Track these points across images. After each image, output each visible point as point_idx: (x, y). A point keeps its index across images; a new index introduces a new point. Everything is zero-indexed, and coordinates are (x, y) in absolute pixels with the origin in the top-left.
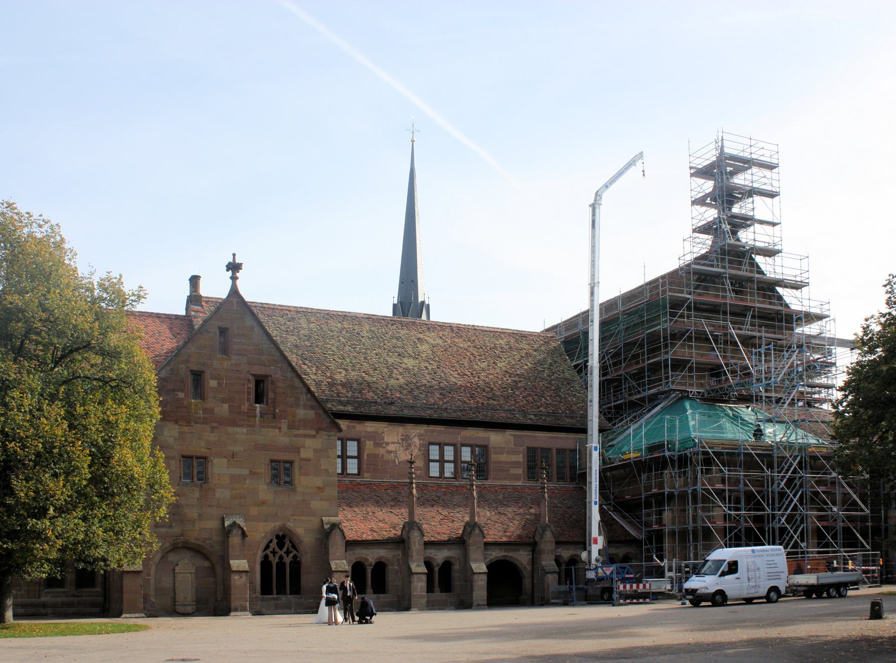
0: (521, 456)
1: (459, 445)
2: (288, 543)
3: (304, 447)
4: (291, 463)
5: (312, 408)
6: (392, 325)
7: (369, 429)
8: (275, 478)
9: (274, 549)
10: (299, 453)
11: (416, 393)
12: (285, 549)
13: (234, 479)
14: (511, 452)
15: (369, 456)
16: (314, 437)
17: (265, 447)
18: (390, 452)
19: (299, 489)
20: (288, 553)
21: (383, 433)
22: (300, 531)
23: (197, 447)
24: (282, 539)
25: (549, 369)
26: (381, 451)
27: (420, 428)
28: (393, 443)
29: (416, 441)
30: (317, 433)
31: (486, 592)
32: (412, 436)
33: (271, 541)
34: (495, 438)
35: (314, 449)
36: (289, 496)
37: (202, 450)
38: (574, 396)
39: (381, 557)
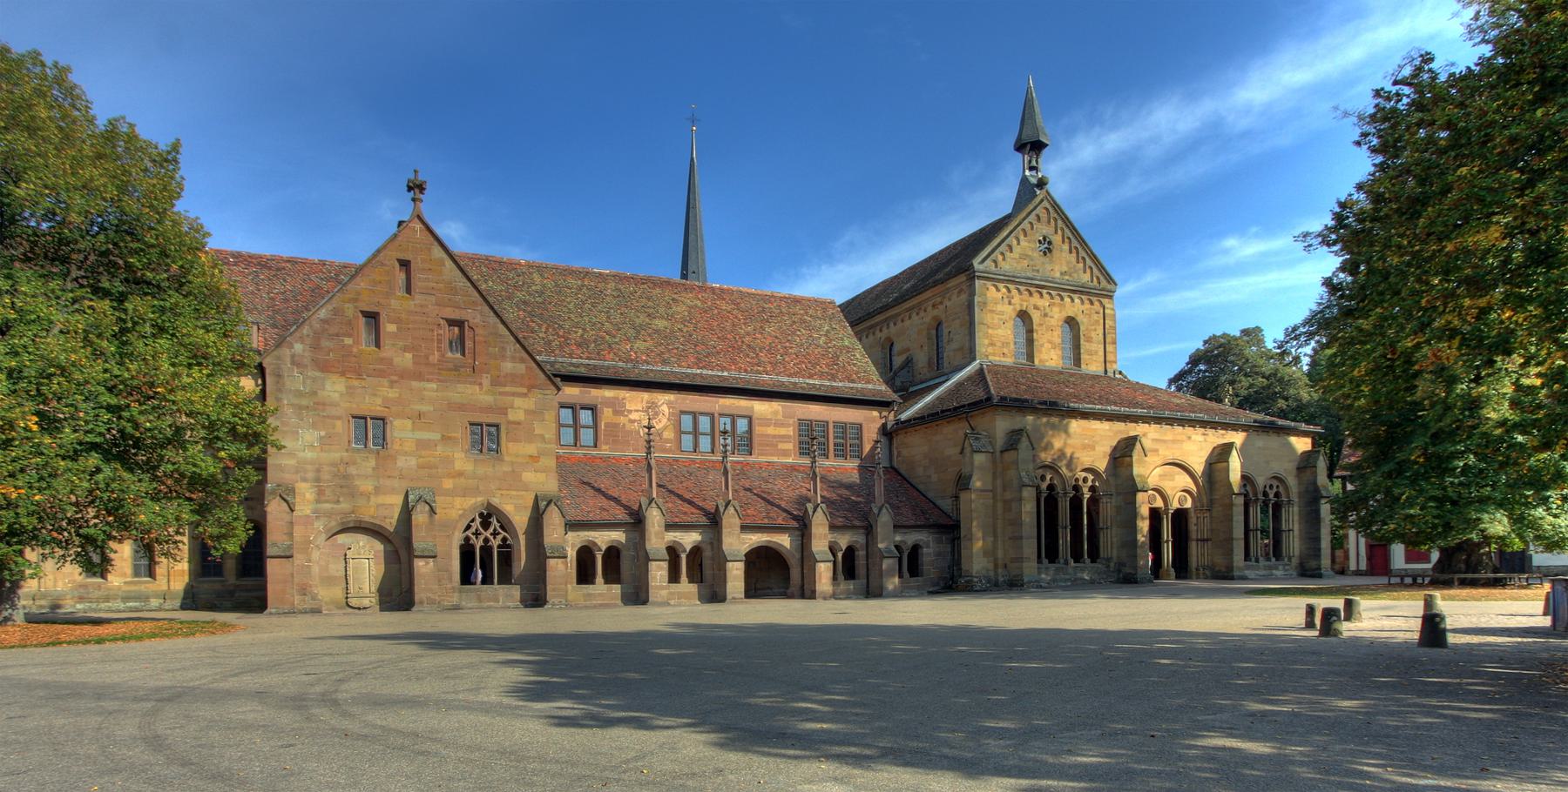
1: (716, 415)
3: (512, 407)
4: (497, 426)
5: (522, 360)
6: (643, 284)
9: (477, 530)
10: (506, 414)
11: (666, 356)
12: (491, 530)
13: (422, 445)
14: (778, 424)
15: (607, 425)
16: (525, 395)
17: (461, 407)
18: (633, 421)
19: (507, 458)
20: (495, 534)
22: (508, 508)
23: (371, 404)
24: (488, 516)
25: (826, 335)
26: (622, 420)
28: (637, 411)
30: (529, 390)
31: (743, 584)
33: (473, 521)
34: (760, 407)
35: (525, 411)
36: (494, 466)
37: (378, 408)
38: (854, 365)
39: (613, 541)
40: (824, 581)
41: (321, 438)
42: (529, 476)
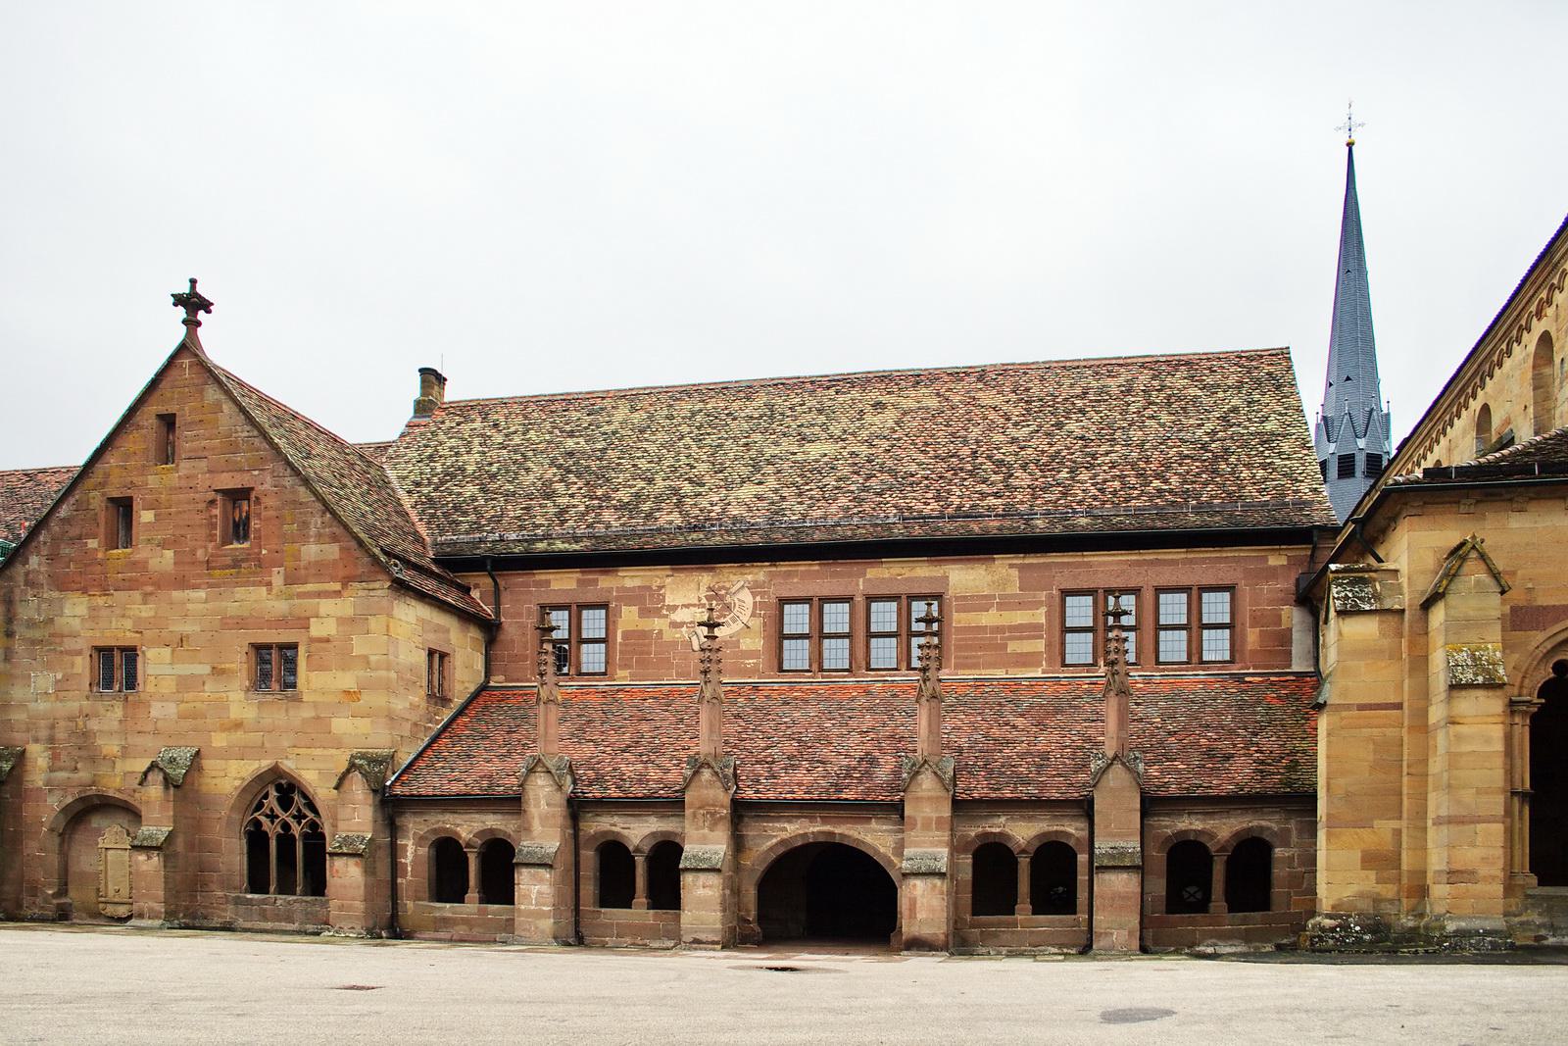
0: (1043, 610)
1: (859, 599)
7: (629, 583)
8: (261, 679)
13: (185, 683)
19: (305, 698)
21: (660, 588)
27: (756, 570)
32: (733, 590)
34: (962, 577)
36: (287, 711)
40: (921, 915)
41: (57, 682)
42: (341, 725)
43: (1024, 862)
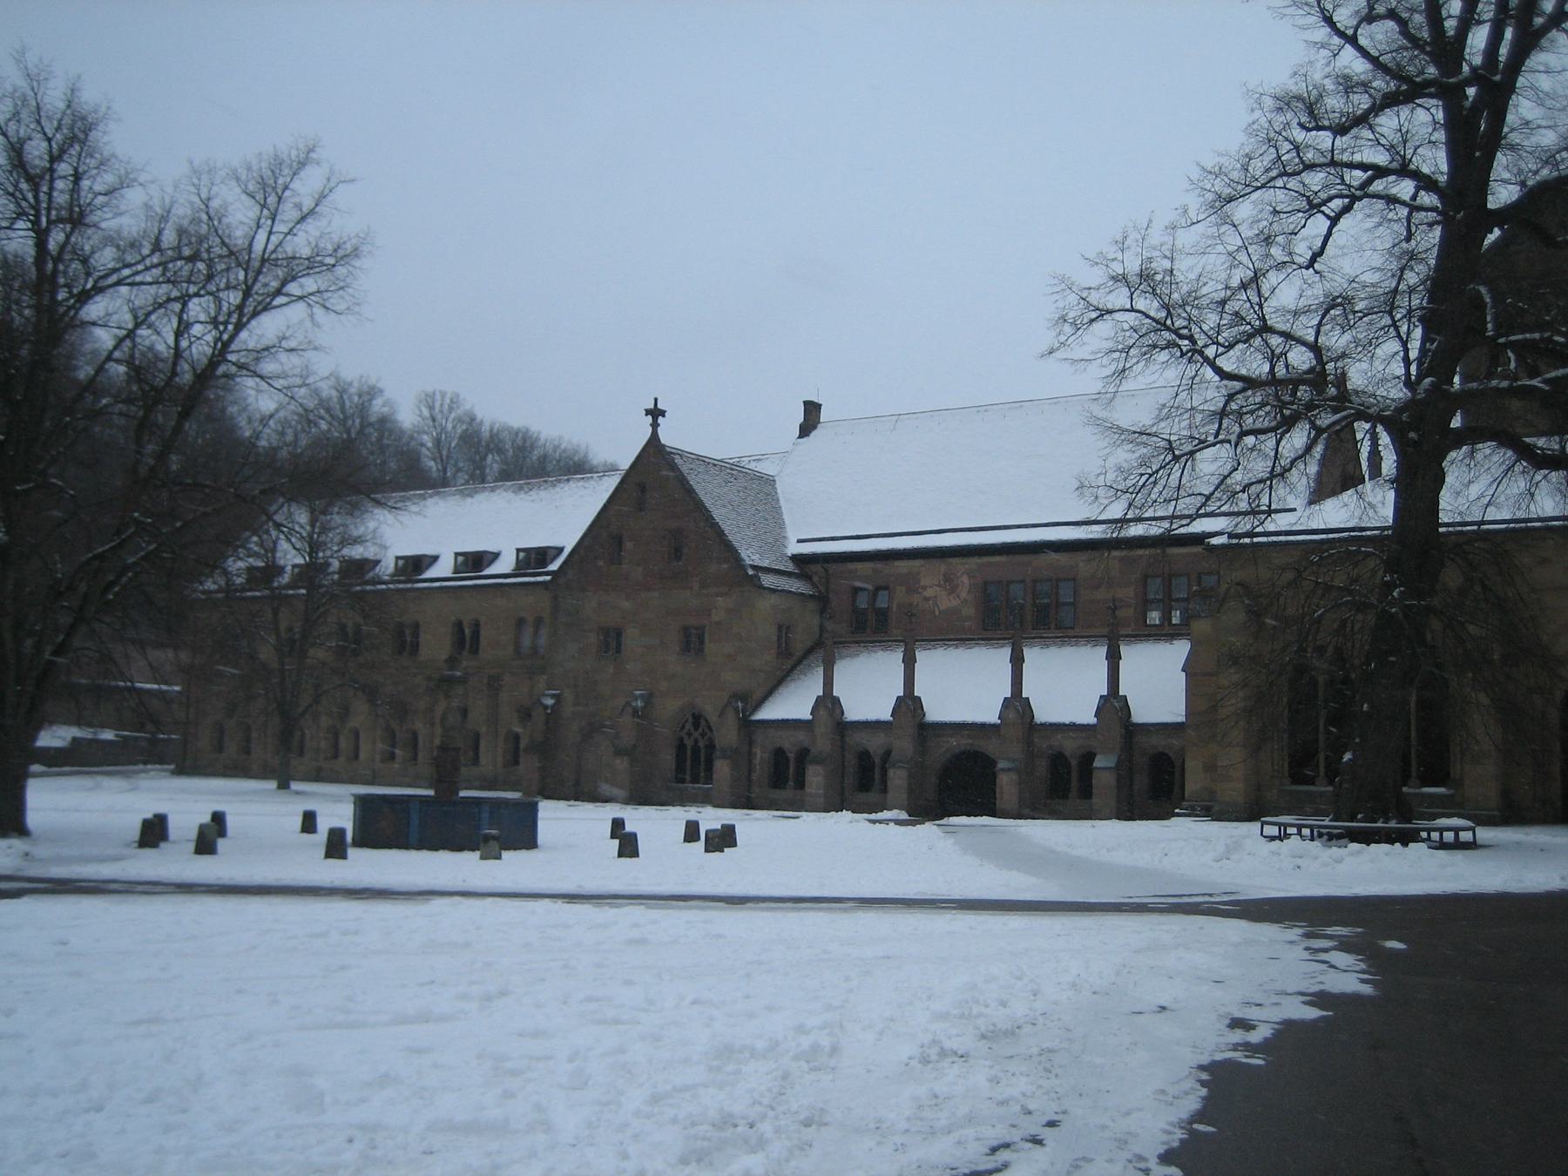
2: (703, 722)
10: (709, 615)
18: (927, 599)
20: (703, 735)
26: (915, 599)
29: (964, 581)
30: (730, 590)
33: (686, 722)
43: (1074, 763)
